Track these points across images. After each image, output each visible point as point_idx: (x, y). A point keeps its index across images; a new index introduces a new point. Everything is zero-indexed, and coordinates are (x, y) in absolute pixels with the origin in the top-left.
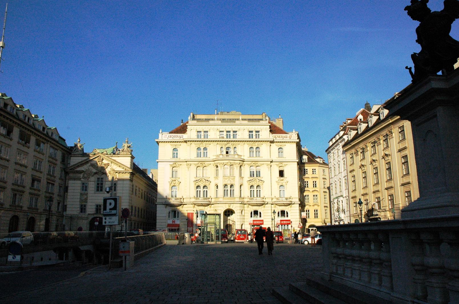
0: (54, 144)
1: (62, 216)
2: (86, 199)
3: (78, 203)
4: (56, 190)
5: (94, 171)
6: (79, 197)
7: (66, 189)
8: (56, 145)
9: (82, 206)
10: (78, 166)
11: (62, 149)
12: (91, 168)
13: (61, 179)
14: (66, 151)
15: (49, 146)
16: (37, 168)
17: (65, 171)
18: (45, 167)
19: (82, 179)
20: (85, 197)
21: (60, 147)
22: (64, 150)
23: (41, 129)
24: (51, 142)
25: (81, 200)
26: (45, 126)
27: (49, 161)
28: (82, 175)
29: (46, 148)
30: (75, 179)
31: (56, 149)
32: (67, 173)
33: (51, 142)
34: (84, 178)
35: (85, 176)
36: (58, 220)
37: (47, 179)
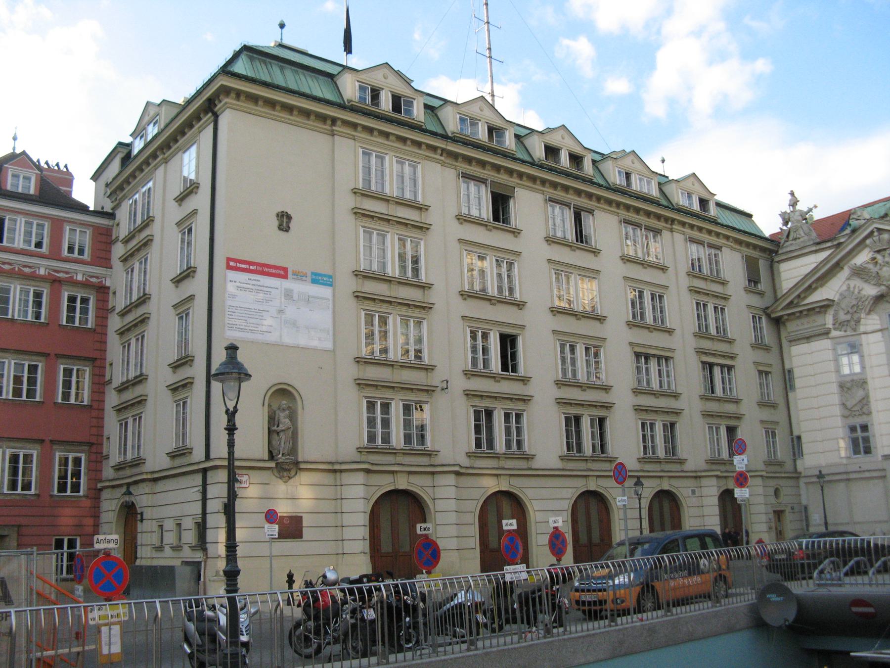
0: (700, 229)
1: (796, 476)
2: (865, 401)
3: (839, 422)
4: (745, 383)
5: (871, 291)
6: (836, 399)
7: (788, 379)
8: (710, 232)
9: (853, 429)
10: (810, 289)
11: (740, 242)
12: (857, 283)
13: (759, 345)
14: (755, 247)
15: (679, 238)
16: (649, 319)
17: (768, 316)
18: (680, 311)
19: (834, 333)
20: (860, 393)
21: (727, 238)
22: (748, 245)
23: (696, 207)
24: (683, 224)
25: (848, 411)
26: (705, 196)
27: (694, 291)
28: (829, 320)
29: (674, 249)
30: (808, 338)
31: (719, 248)
32: (777, 322)
33: (683, 224)
34: (840, 325)
35: (842, 317)
36: (777, 492)
37: (700, 352)
